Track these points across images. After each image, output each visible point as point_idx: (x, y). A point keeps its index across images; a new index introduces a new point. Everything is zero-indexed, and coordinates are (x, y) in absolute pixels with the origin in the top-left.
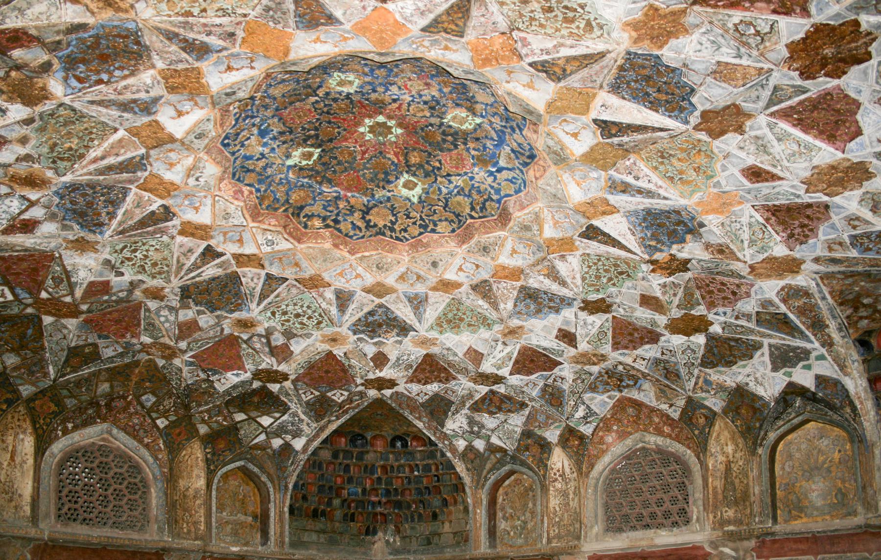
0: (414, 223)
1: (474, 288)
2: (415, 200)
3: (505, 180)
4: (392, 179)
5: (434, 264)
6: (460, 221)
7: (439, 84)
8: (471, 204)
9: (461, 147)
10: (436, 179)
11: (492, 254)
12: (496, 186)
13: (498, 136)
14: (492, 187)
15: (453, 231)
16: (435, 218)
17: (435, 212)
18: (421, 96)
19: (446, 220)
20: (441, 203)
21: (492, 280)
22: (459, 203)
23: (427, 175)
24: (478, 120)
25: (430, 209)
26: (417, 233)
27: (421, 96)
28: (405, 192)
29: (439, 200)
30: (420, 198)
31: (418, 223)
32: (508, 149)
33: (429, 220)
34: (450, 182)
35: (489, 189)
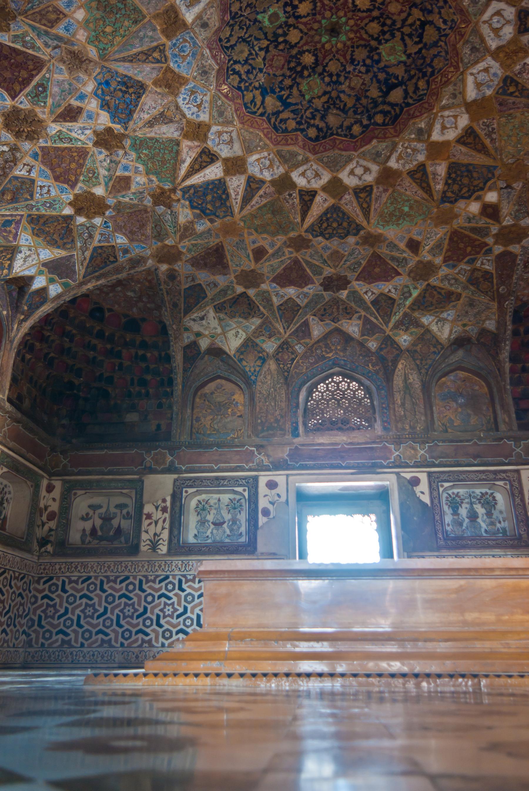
0: (241, 9)
1: (161, 49)
2: (259, 17)
3: (254, 97)
4: (289, 9)
5: (205, 25)
6: (227, 48)
7: (349, 96)
8: (239, 62)
9: (288, 73)
10: (268, 40)
11: (199, 78)
12: (251, 88)
13: (290, 104)
14: (250, 84)
15: (220, 40)
16: (237, 27)
17: (241, 28)
18: (346, 78)
19: (231, 35)
20: (247, 36)
21: (164, 66)
22: (242, 52)
23: (276, 36)
24: (307, 97)
25: (245, 25)
26: (233, 9)
27: (346, 78)
28: (271, 11)
29: (250, 36)
30: (260, 22)
31: (239, 12)
32: (281, 109)
33: (236, 22)
34: (261, 49)
35: (250, 81)
